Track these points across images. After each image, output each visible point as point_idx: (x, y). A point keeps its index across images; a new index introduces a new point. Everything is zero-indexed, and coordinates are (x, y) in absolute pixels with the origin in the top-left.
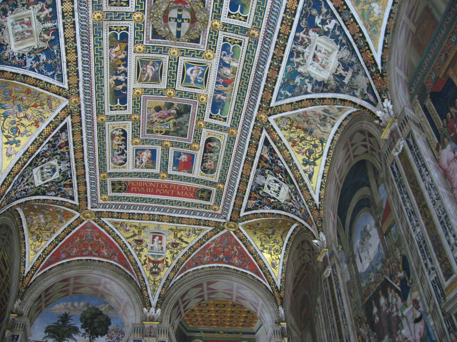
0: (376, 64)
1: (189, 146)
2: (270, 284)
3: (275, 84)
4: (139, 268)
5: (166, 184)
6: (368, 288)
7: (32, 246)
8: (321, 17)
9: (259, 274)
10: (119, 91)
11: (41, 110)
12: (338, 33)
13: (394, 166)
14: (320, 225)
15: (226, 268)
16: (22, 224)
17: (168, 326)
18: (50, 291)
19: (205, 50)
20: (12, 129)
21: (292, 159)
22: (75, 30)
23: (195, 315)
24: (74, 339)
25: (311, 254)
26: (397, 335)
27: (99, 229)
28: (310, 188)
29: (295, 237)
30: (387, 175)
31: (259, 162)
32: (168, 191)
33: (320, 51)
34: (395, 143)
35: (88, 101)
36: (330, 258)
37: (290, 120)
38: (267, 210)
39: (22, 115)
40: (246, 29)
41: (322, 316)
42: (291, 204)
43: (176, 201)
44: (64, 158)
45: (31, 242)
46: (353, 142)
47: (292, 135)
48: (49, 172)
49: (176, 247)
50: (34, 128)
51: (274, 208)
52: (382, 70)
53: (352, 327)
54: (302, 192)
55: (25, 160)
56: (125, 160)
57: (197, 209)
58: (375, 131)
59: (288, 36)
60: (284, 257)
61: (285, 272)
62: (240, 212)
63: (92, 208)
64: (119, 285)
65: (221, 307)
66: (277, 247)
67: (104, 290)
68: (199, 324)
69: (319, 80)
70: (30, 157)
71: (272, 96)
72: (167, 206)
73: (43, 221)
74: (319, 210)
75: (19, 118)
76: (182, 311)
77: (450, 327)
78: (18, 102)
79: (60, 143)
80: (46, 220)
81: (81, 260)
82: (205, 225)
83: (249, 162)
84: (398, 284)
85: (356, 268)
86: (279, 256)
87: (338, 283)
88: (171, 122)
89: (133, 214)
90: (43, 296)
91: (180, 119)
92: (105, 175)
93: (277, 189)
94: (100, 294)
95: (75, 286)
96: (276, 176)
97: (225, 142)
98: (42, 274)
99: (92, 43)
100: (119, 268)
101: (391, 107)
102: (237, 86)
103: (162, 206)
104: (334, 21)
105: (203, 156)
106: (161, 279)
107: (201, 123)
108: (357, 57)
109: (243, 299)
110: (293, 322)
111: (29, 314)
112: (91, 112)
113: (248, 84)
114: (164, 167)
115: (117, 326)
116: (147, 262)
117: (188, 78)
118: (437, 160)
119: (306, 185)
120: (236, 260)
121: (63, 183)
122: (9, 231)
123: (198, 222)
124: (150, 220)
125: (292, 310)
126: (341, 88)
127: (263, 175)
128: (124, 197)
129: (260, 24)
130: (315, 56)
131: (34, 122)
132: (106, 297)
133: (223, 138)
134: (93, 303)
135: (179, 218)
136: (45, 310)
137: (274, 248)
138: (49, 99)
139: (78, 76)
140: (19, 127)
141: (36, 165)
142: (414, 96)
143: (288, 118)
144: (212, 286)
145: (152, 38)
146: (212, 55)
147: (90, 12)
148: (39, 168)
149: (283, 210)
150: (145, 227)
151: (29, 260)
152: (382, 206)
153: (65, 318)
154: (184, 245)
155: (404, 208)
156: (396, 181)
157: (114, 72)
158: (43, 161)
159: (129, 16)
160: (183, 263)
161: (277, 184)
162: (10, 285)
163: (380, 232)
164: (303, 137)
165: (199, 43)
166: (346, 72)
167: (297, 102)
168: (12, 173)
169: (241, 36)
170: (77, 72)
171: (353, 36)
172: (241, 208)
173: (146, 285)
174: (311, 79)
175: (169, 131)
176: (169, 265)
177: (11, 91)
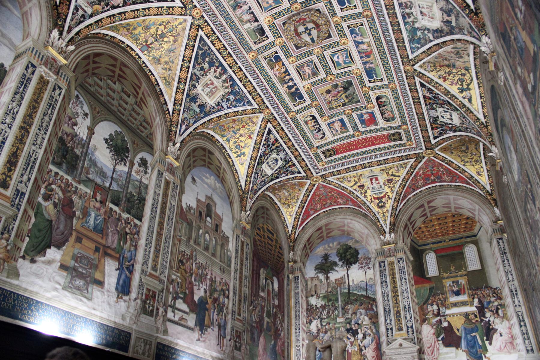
1: (365, 107)
3: (404, 42)
9: (469, 184)
10: (294, 92)
11: (248, 127)
15: (441, 185)
16: (273, 200)
18: (311, 240)
19: (339, 39)
20: (236, 147)
21: (448, 92)
22: (242, 71)
23: (423, 232)
28: (473, 110)
31: (425, 101)
33: (423, 8)
35: (276, 108)
37: (431, 63)
38: (451, 134)
39: (238, 136)
42: (464, 126)
44: (279, 150)
45: (285, 210)
49: (392, 182)
50: (249, 140)
51: (455, 131)
52: (475, 8)
55: (253, 163)
56: (324, 134)
59: (393, 5)
60: (486, 164)
62: (430, 141)
64: (359, 222)
65: (443, 220)
66: (475, 158)
69: (435, 29)
70: (256, 160)
71: (406, 51)
72: (371, 154)
73: (287, 194)
74: (486, 127)
76: (412, 231)
78: (232, 129)
82: (407, 159)
83: (417, 103)
86: (481, 164)
89: (348, 168)
91: (349, 92)
93: (449, 117)
94: (346, 233)
96: (443, 107)
97: (391, 95)
99: (258, 72)
102: (377, 53)
105: (380, 111)
106: (388, 210)
112: (283, 114)
113: (384, 49)
114: (355, 128)
116: (373, 200)
117: (338, 62)
119: (468, 109)
120: (446, 178)
121: (287, 166)
122: (265, 210)
123: (401, 158)
130: (421, 13)
133: (388, 93)
134: (343, 241)
136: (311, 255)
139: (260, 96)
141: (263, 163)
143: (429, 62)
144: (431, 204)
146: (346, 41)
147: (246, 55)
148: (265, 163)
153: (326, 257)
154: (397, 179)
157: (284, 82)
158: (266, 158)
159: (273, 44)
160: (402, 192)
161: (447, 113)
164: (449, 71)
165: (331, 37)
167: (427, 50)
169: (359, 20)
170: (259, 94)
172: (429, 138)
174: (428, 30)
176: (391, 197)
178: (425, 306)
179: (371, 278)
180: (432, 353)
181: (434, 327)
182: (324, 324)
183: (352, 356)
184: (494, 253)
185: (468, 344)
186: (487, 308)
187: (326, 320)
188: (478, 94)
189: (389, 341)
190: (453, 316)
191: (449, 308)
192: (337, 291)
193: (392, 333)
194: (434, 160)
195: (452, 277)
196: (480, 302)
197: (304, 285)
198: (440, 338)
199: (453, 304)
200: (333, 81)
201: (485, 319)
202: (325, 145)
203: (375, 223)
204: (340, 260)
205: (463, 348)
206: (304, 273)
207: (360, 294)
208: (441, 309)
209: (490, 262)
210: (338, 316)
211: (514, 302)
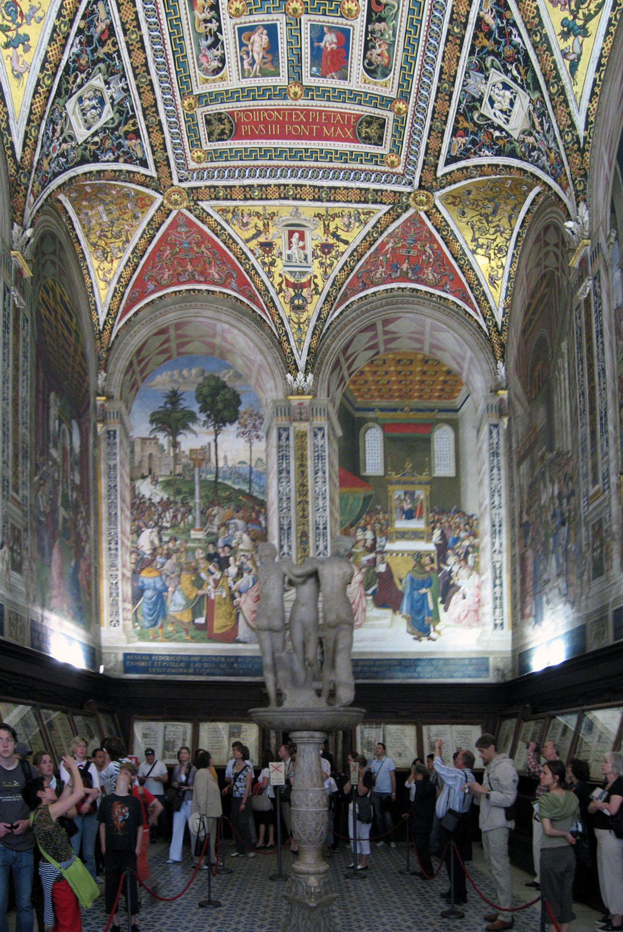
14: (580, 188)
18: (144, 353)
24: (194, 432)
29: (534, 217)
32: (305, 125)
36: (593, 261)
68: (372, 397)
81: (180, 291)
87: (601, 311)
90: (135, 363)
98: (126, 323)
106: (308, 319)
111: (121, 394)
135: (330, 188)
136: (142, 386)
137: (495, 244)
153: (174, 397)
162: (84, 348)
173: (286, 331)
182: (165, 539)
183: (216, 606)
187: (169, 531)
192: (193, 476)
197: (128, 453)
203: (279, 343)
204: (202, 410)
206: (128, 425)
210: (192, 526)
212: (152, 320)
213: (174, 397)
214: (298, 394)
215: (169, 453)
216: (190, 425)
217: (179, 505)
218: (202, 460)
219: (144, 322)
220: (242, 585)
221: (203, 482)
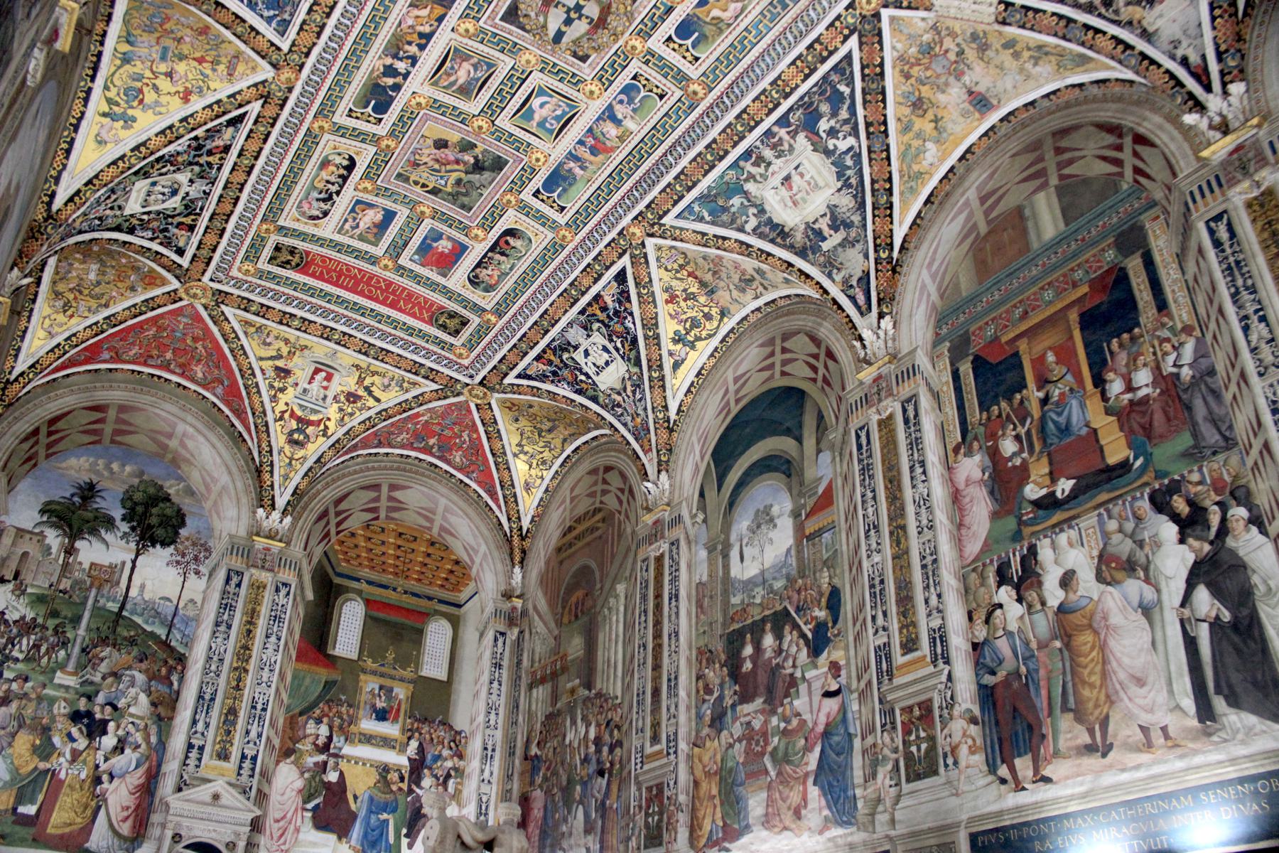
0: (891, 245)
1: (466, 230)
2: (509, 519)
3: (689, 189)
4: (267, 425)
5: (385, 280)
6: (744, 610)
7: (47, 322)
8: (832, 122)
9: (493, 495)
10: (384, 88)
11: (208, 72)
12: (849, 162)
13: (863, 434)
15: (432, 464)
17: (300, 556)
18: (60, 425)
21: (656, 325)
23: (356, 546)
25: (624, 499)
26: (782, 705)
27: (206, 325)
28: (668, 386)
30: (844, 442)
31: (589, 304)
33: (802, 175)
34: (880, 400)
39: (163, 68)
40: (686, 78)
41: (621, 620)
42: (619, 398)
43: (389, 317)
45: (47, 311)
46: (787, 345)
47: (674, 283)
48: (163, 194)
49: (354, 402)
50: (176, 101)
51: (579, 392)
53: (689, 660)
54: (651, 387)
56: (326, 214)
57: (424, 344)
58: (844, 356)
59: (757, 124)
60: (553, 478)
61: (543, 505)
62: (506, 375)
63: (211, 280)
64: (214, 446)
66: (547, 455)
67: (180, 449)
69: (775, 221)
71: (673, 206)
72: (367, 321)
73: (92, 276)
74: (671, 430)
75: (153, 72)
76: (333, 531)
77: (885, 724)
79: (214, 144)
80: (100, 278)
81: (139, 372)
82: (426, 378)
84: (810, 626)
85: (726, 567)
86: (545, 473)
88: (455, 175)
89: (292, 315)
90: (44, 431)
91: (475, 178)
92: (272, 228)
93: (601, 362)
94: (170, 456)
95: (117, 427)
96: (611, 340)
100: (219, 409)
101: (891, 332)
103: (359, 318)
104: (851, 141)
106: (305, 458)
107: (512, 199)
108: (864, 219)
109: (452, 534)
110: (542, 604)
112: (307, 108)
114: (396, 250)
115: (199, 532)
116: (287, 416)
117: (531, 111)
118: (949, 469)
119: (662, 379)
120: (457, 457)
123: (416, 369)
124: (321, 336)
125: (544, 581)
126: (810, 253)
127: (585, 328)
128: (287, 278)
129: (717, 81)
130: (787, 178)
131: (181, 89)
132: (183, 466)
133: (541, 238)
134: (154, 472)
136: (43, 464)
138: (237, 57)
139: (319, 35)
140: (145, 89)
141: (146, 175)
142: (944, 341)
144: (397, 494)
145: (502, 19)
146: (597, 92)
148: (150, 180)
149: (597, 403)
150: (306, 347)
151: (30, 347)
152: (817, 487)
153: (89, 491)
154: (371, 402)
155: (860, 513)
156: (860, 461)
158: (164, 170)
161: (606, 356)
163: (799, 529)
166: (832, 232)
167: (715, 236)
168: (95, 181)
169: (669, 85)
171: (873, 182)
174: (762, 211)
175: (440, 190)
176: (330, 433)
177: (168, 19)
178: (302, 719)
179: (192, 601)
180: (281, 836)
181: (307, 775)
184: (480, 658)
185: (365, 835)
186: (430, 768)
187: (20, 666)
188: (699, 365)
189: (186, 777)
190: (356, 763)
191: (352, 742)
192: (86, 598)
193: (200, 760)
194: (470, 411)
195: (382, 675)
196: (421, 749)
198: (310, 806)
199: (365, 735)
200: (478, 135)
201: (418, 791)
202: (302, 236)
205: (353, 843)
207: (149, 629)
208: (335, 739)
209: (467, 673)
210: (62, 667)
211: (482, 771)
212: (87, 390)
213: (89, 491)
214: (269, 537)
215: (57, 560)
216: (103, 532)
217: (50, 632)
218: (107, 581)
219: (74, 388)
220: (117, 767)
221: (98, 611)
